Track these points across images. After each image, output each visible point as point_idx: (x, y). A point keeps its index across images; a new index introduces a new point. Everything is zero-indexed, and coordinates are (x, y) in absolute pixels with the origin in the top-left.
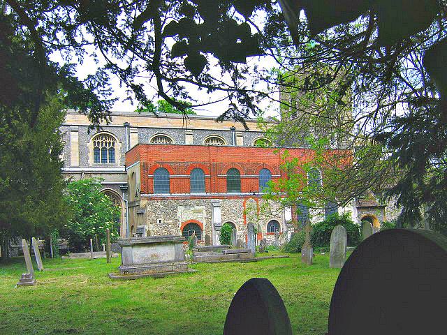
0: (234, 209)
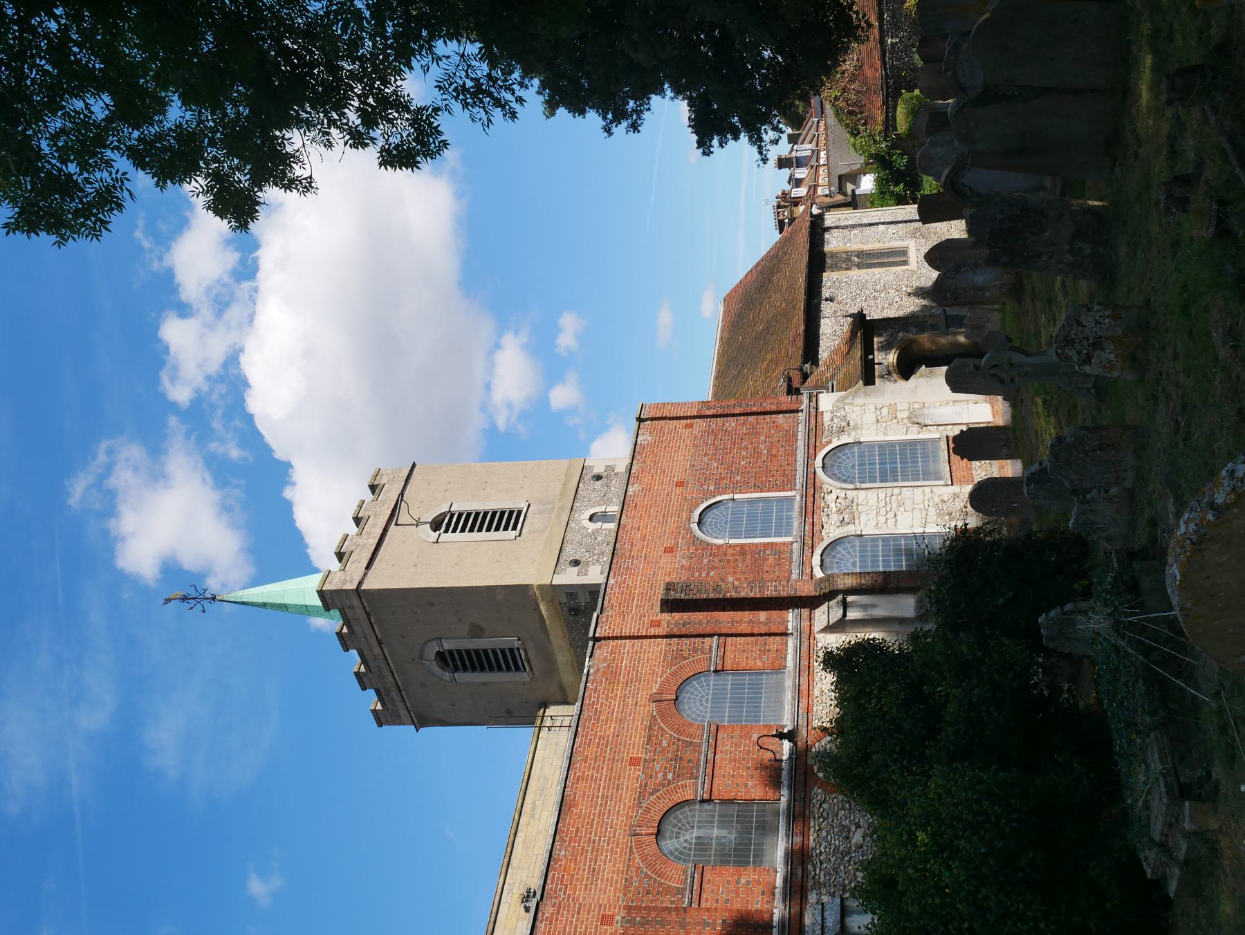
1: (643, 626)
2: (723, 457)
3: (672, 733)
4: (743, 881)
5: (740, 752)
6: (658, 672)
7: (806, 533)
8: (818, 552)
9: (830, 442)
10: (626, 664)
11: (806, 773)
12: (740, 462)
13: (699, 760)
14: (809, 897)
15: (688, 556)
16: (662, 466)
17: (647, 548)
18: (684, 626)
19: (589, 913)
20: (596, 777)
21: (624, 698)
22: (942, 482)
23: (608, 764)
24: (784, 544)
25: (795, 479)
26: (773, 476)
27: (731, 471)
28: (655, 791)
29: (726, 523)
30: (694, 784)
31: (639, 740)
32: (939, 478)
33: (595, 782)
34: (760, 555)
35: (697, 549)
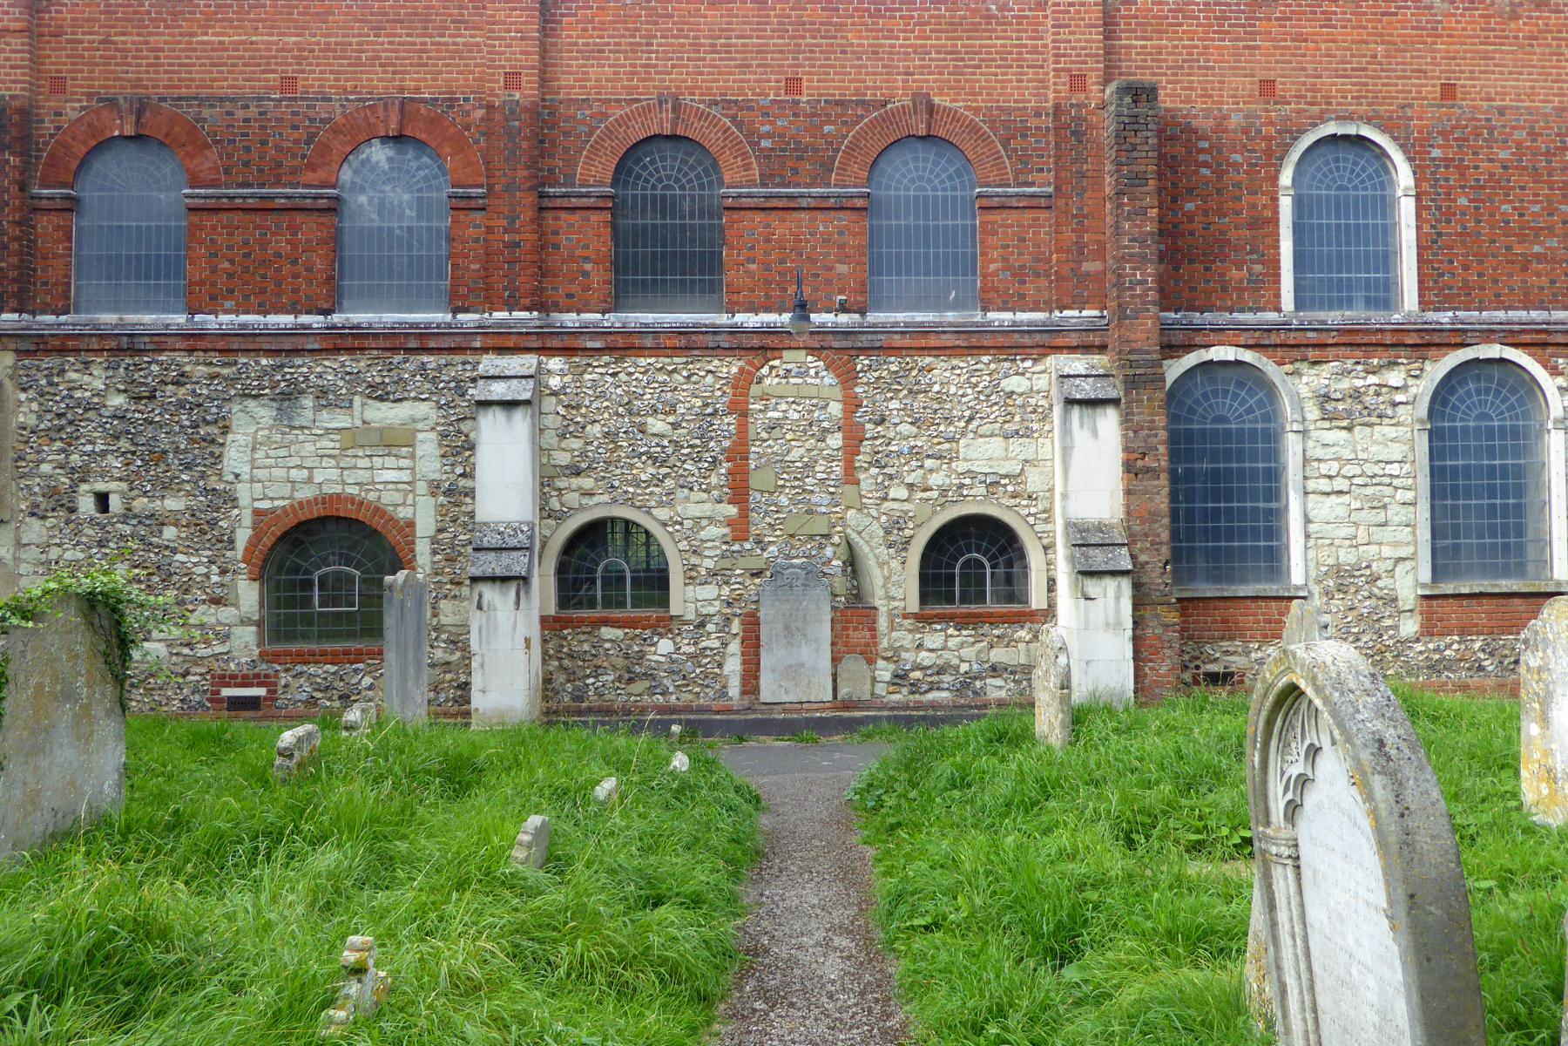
0: (657, 425)
1: (1071, 62)
2: (1525, 168)
3: (849, 138)
4: (588, 266)
5: (814, 248)
6: (977, 101)
7: (1297, 334)
8: (1248, 356)
9: (1555, 371)
10: (995, 46)
11: (764, 348)
12: (1509, 202)
13: (797, 185)
14: (557, 359)
15: (1252, 124)
16: (1502, 52)
17: (1275, 48)
18: (1074, 133)
19: (522, 53)
20: (765, 30)
21: (922, 51)
22: (1425, 574)
23: (789, 45)
24: (1278, 296)
25: (1455, 309)
26: (1466, 268)
27: (1483, 188)
28: (739, 125)
29: (1340, 188)
30: (751, 184)
31: (835, 88)
32: (1438, 573)
33: (754, 30)
34: (1251, 253)
35: (1269, 139)
